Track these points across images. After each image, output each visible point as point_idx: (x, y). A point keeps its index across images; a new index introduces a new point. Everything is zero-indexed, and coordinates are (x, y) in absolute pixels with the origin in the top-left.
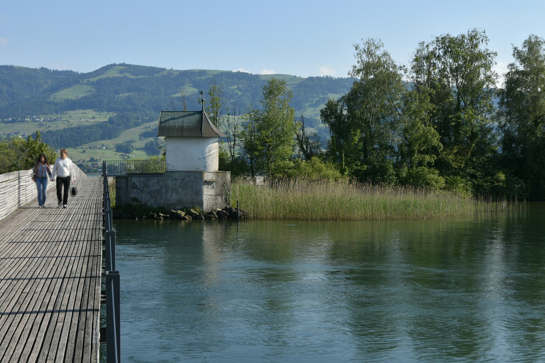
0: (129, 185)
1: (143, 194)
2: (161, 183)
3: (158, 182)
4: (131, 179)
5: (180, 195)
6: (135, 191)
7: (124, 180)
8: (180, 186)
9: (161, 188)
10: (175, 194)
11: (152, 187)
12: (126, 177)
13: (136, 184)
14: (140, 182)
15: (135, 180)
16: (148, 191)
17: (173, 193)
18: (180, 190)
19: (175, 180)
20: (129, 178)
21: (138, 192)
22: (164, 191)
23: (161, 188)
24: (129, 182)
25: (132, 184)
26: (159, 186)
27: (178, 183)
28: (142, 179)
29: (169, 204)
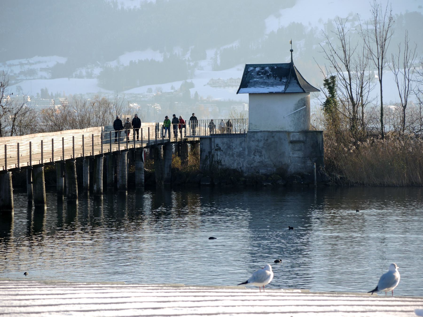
0: (213, 147)
1: (226, 157)
2: (243, 144)
3: (241, 143)
4: (214, 140)
5: (263, 158)
6: (219, 153)
7: (208, 141)
8: (263, 148)
9: (244, 149)
10: (258, 157)
11: (235, 149)
12: (209, 138)
13: (219, 146)
14: (223, 143)
15: (218, 141)
16: (231, 153)
17: (256, 156)
18: (264, 152)
19: (258, 141)
20: (213, 139)
21: (222, 154)
22: (246, 153)
23: (244, 149)
24: (213, 144)
25: (215, 145)
26: (242, 147)
27: (261, 144)
28: (225, 140)
29: (252, 167)
